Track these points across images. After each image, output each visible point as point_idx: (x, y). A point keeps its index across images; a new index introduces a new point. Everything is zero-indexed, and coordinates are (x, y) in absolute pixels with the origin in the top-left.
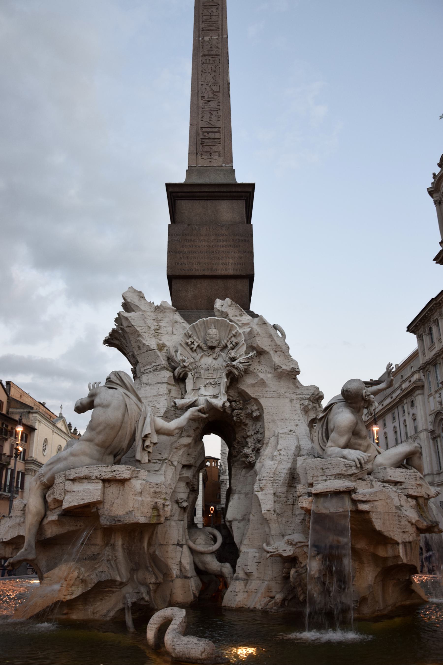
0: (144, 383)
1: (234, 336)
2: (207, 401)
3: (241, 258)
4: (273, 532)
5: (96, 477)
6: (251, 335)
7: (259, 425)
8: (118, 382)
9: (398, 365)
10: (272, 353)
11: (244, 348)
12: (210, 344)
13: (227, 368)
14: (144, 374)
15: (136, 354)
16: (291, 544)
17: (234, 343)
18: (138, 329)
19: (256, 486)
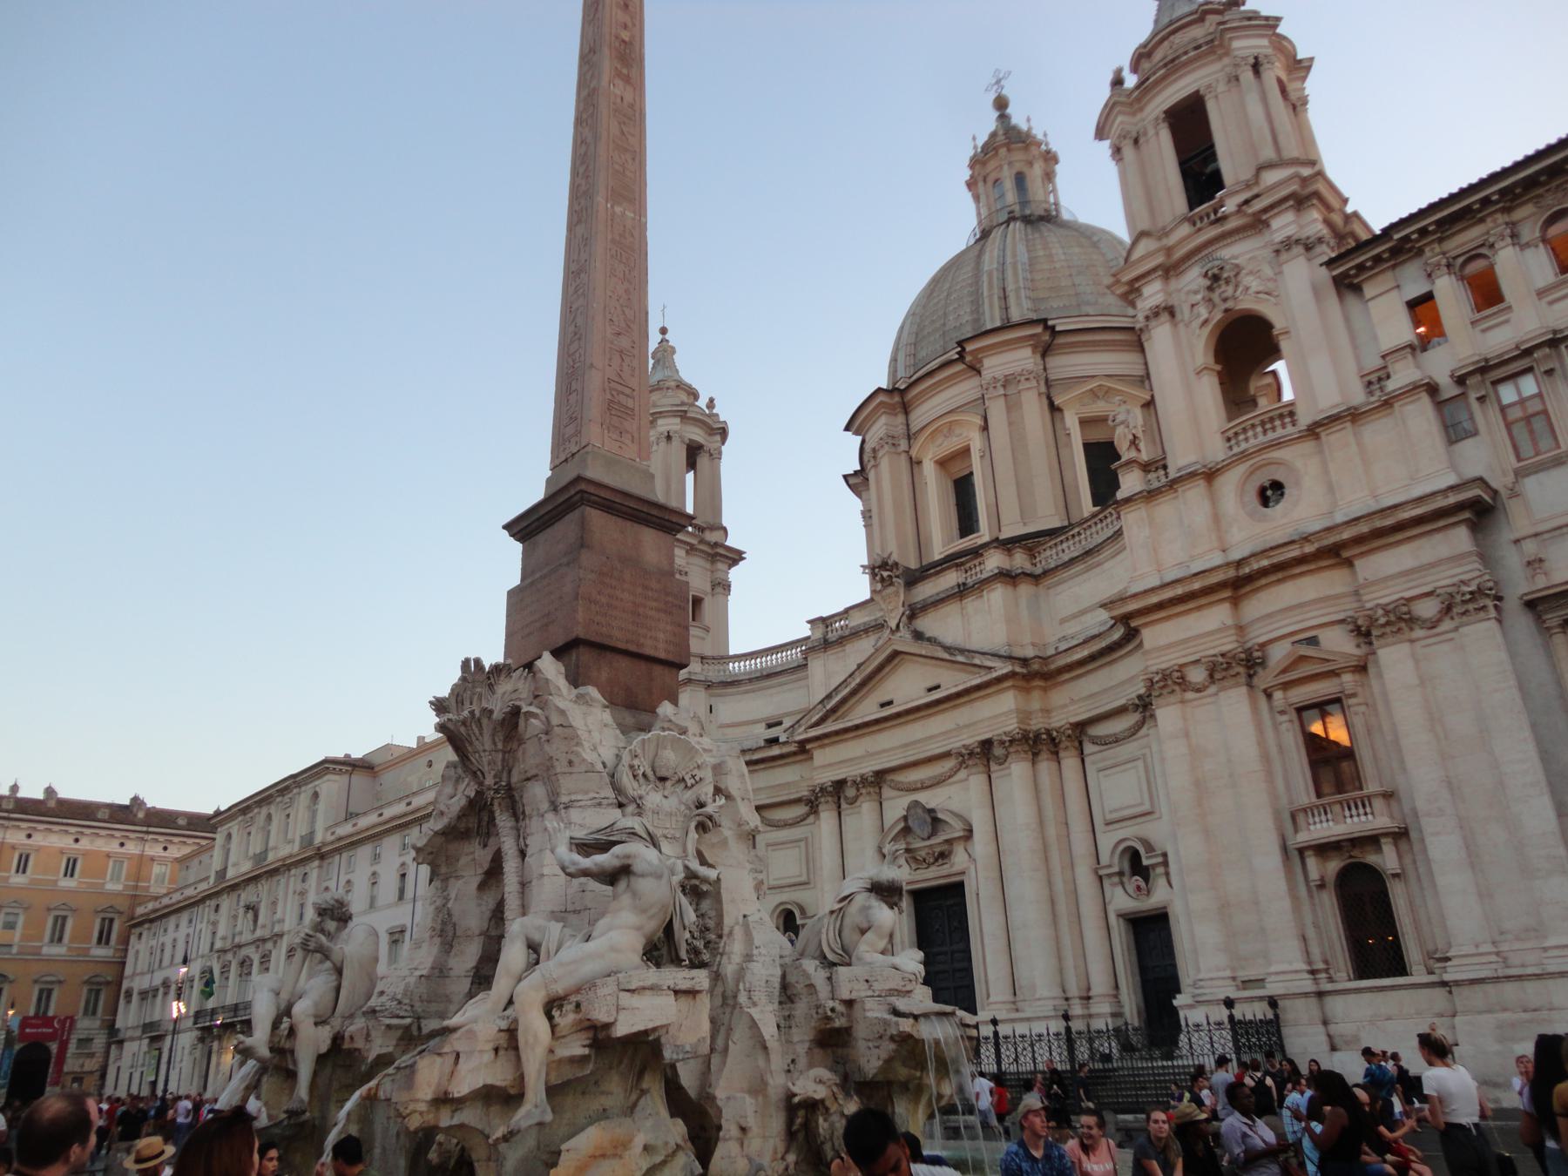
0: (575, 824)
1: (698, 767)
2: (686, 867)
3: (675, 635)
4: (773, 1067)
5: (669, 987)
6: (718, 769)
7: (706, 905)
8: (645, 836)
9: (424, 738)
10: (739, 800)
11: (711, 790)
12: (663, 773)
13: (697, 818)
14: (576, 807)
15: (558, 770)
16: (820, 1082)
17: (697, 778)
18: (579, 733)
19: (742, 998)
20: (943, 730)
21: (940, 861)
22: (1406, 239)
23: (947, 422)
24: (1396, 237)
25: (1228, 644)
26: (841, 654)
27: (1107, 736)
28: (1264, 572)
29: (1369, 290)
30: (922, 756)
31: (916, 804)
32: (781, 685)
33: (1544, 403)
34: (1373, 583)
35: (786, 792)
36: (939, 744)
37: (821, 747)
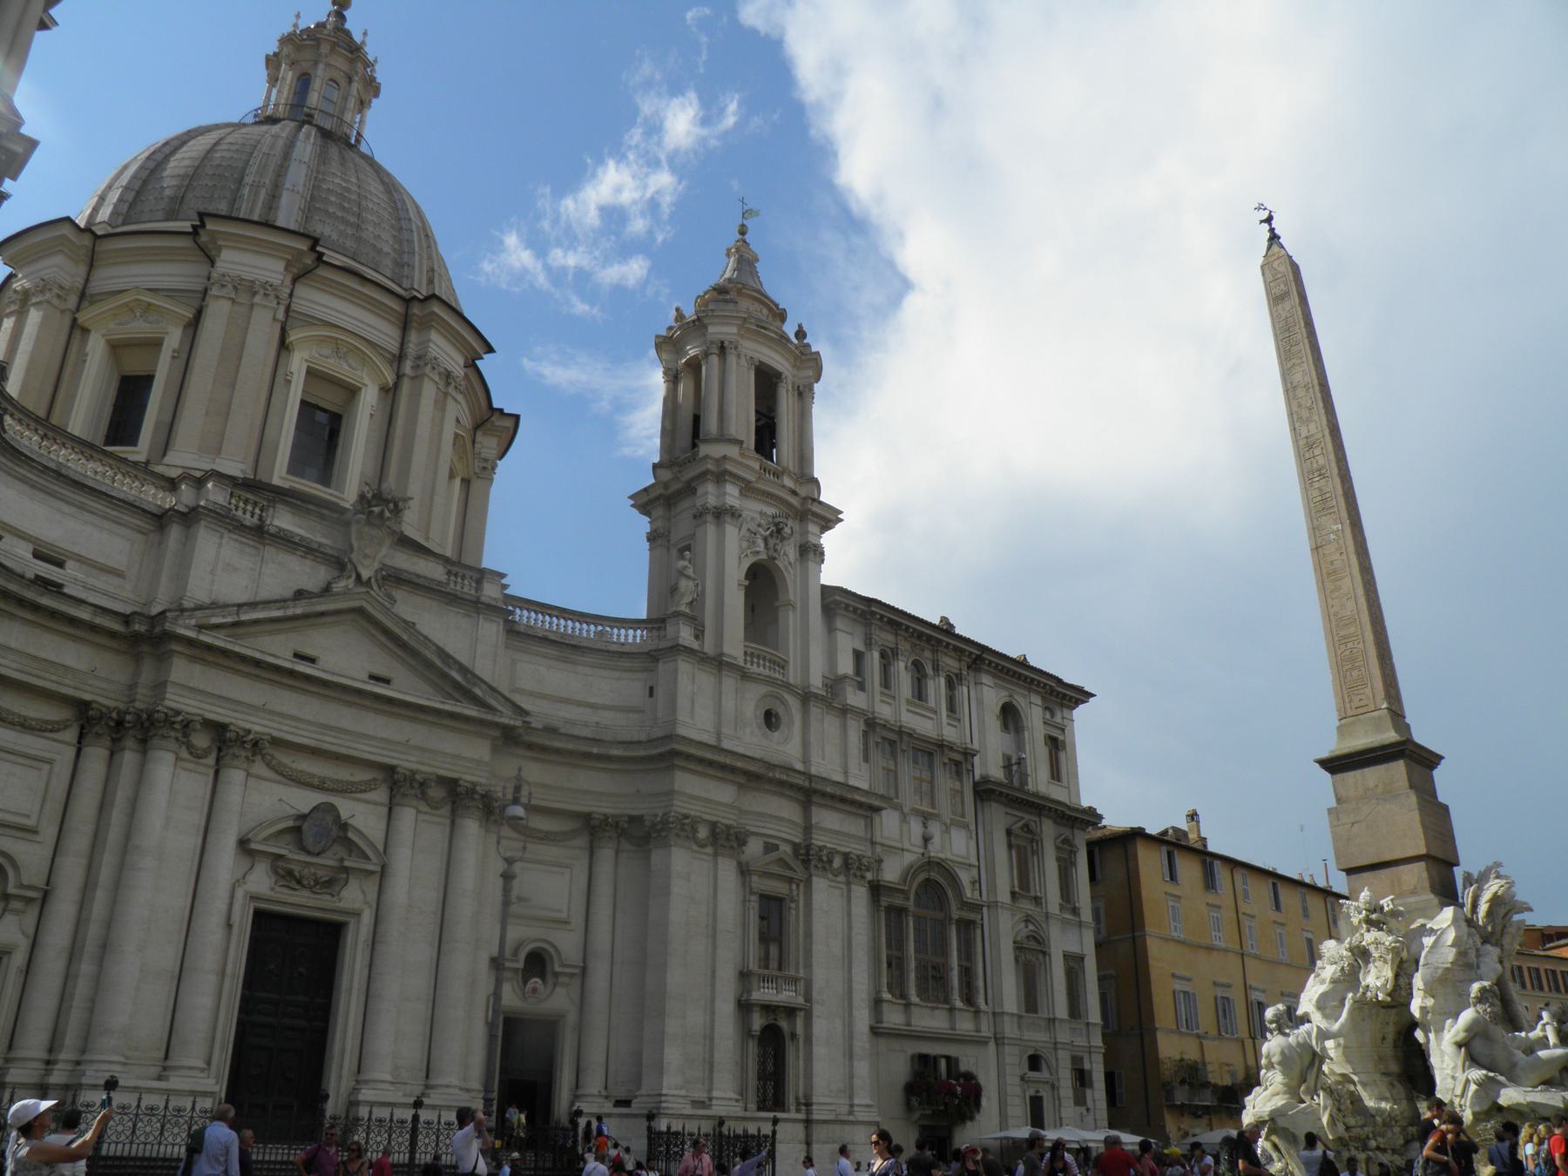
20: (384, 735)
21: (317, 889)
22: (874, 613)
23: (340, 339)
24: (874, 609)
25: (728, 819)
26: (248, 550)
27: (535, 829)
28: (770, 781)
29: (840, 623)
30: (344, 751)
31: (331, 809)
32: (82, 507)
33: (896, 765)
34: (821, 829)
35: (54, 678)
36: (371, 749)
37: (193, 659)
